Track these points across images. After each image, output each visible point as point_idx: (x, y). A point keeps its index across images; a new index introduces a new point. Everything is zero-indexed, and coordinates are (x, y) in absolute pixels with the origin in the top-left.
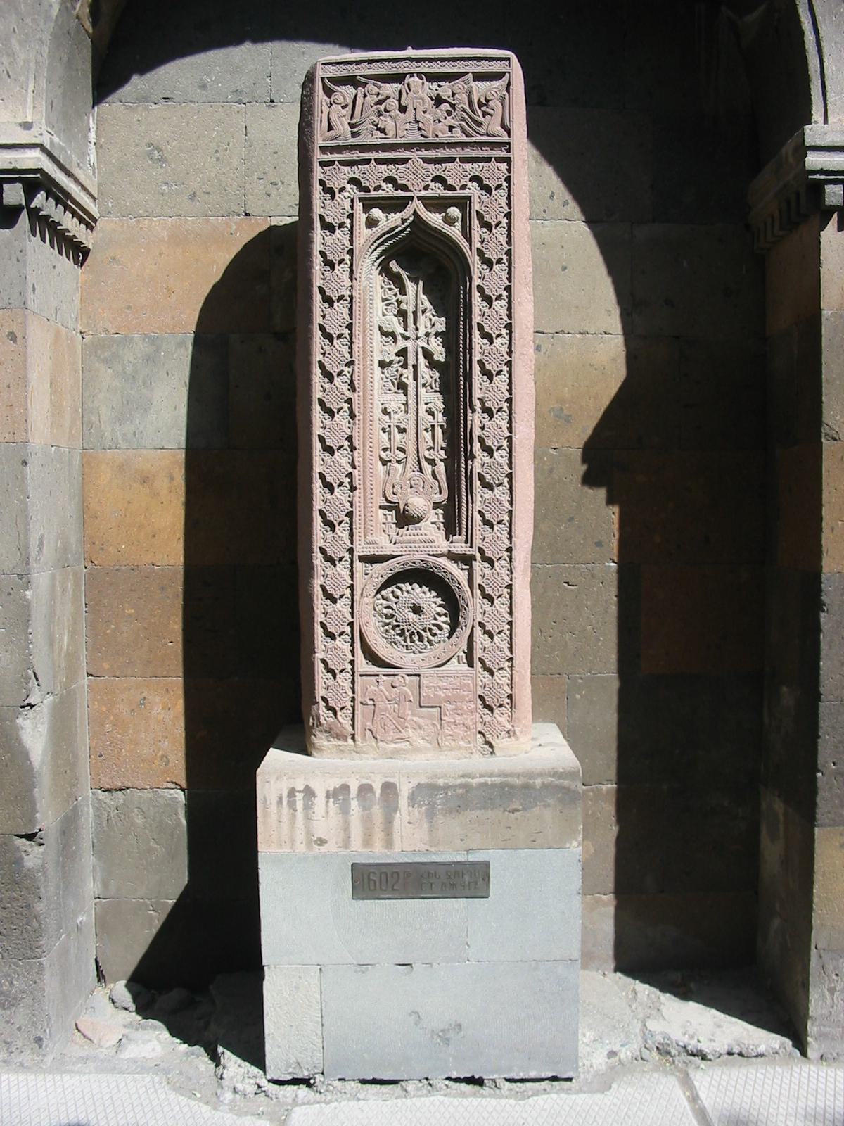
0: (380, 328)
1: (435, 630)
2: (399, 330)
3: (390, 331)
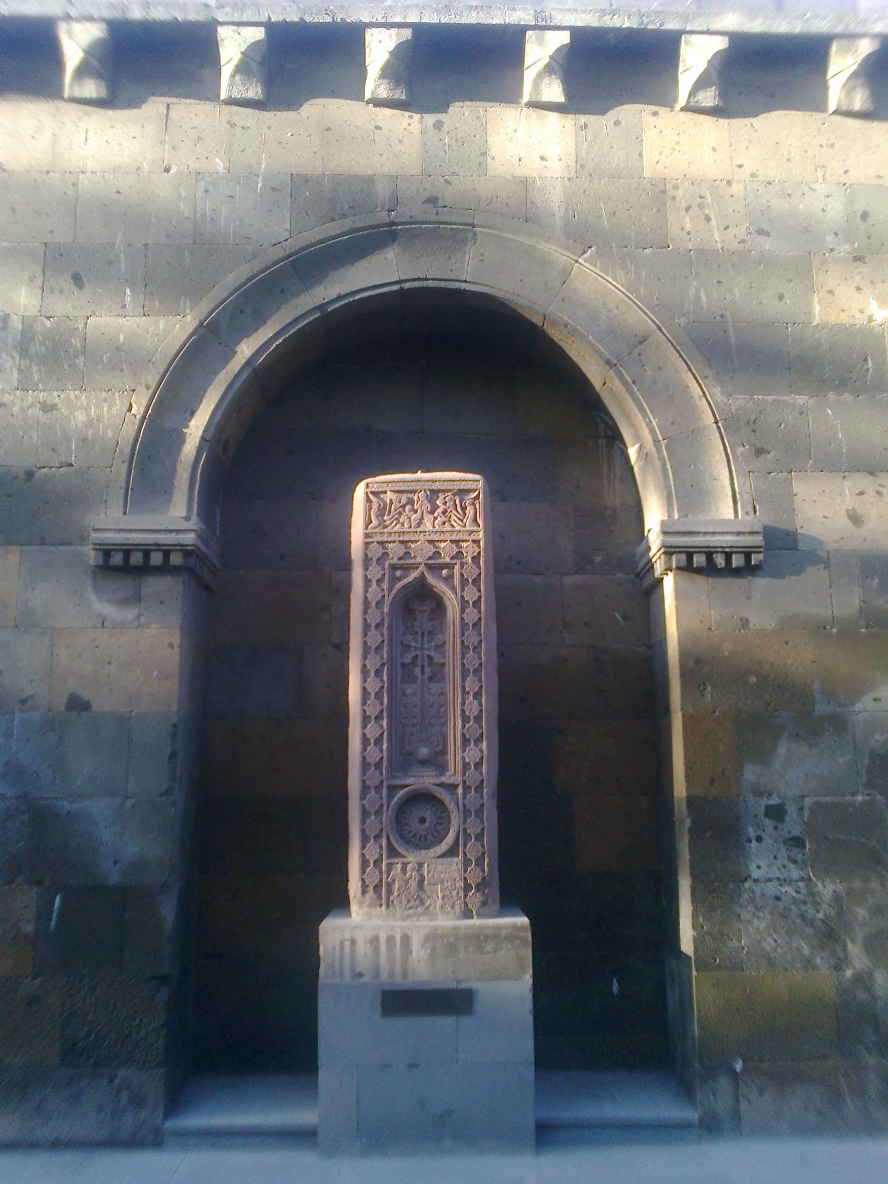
0: (402, 643)
1: (435, 834)
2: (413, 644)
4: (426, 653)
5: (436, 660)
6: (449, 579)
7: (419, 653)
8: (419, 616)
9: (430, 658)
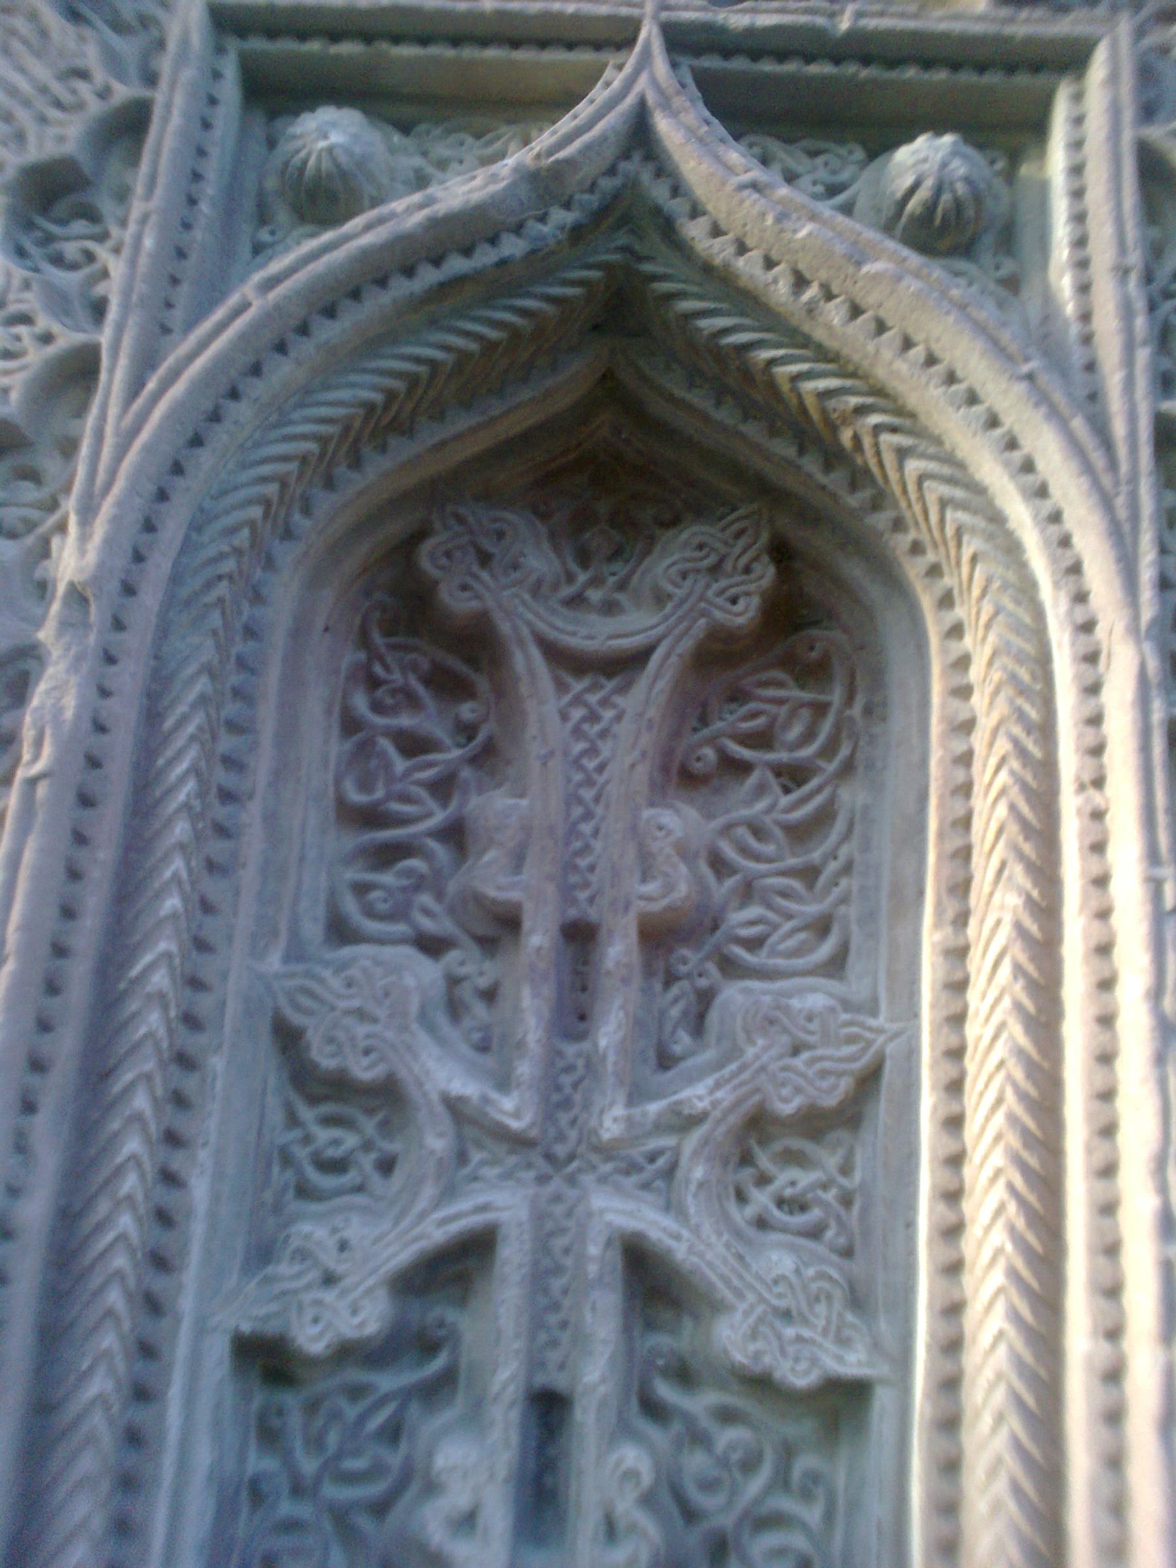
0: (288, 1038)
2: (442, 1073)
3: (364, 1071)
4: (619, 1209)
5: (732, 1337)
6: (967, 235)
7: (503, 1201)
8: (544, 707)
9: (652, 1284)
